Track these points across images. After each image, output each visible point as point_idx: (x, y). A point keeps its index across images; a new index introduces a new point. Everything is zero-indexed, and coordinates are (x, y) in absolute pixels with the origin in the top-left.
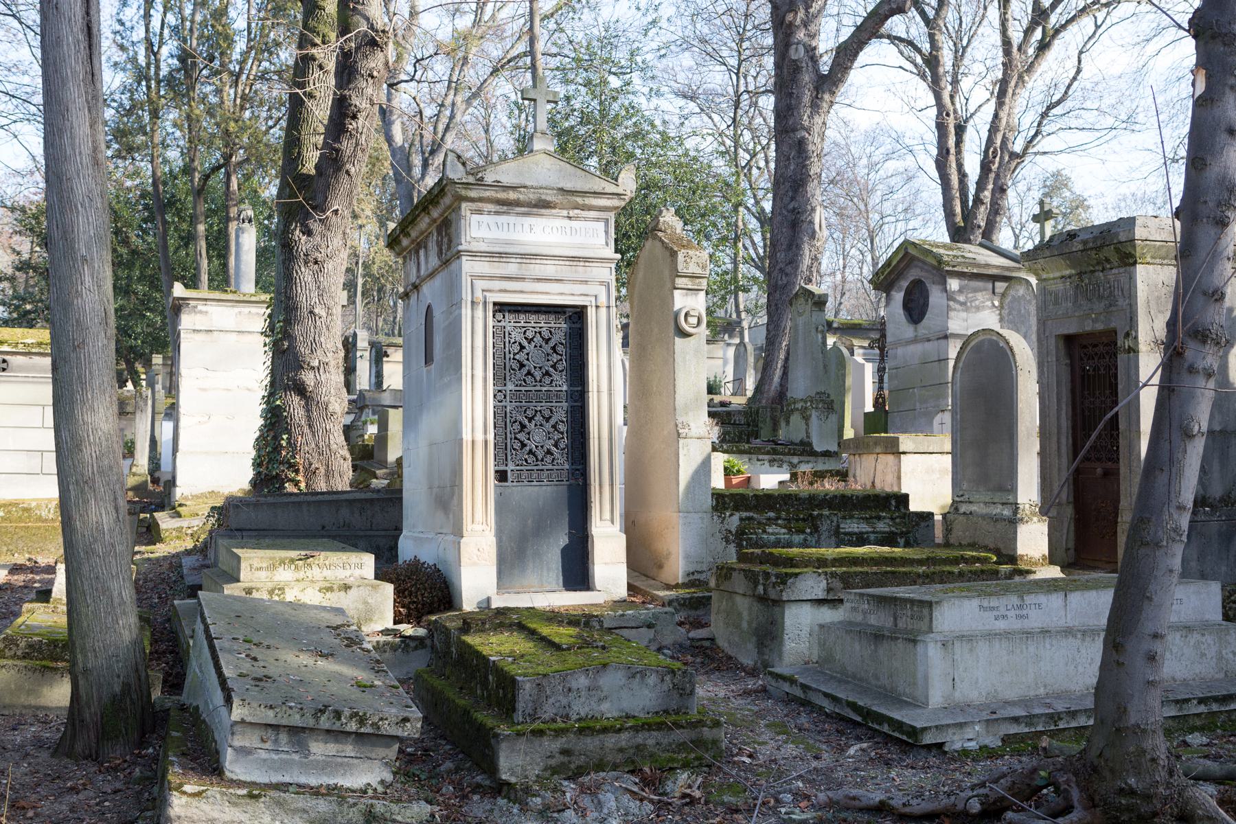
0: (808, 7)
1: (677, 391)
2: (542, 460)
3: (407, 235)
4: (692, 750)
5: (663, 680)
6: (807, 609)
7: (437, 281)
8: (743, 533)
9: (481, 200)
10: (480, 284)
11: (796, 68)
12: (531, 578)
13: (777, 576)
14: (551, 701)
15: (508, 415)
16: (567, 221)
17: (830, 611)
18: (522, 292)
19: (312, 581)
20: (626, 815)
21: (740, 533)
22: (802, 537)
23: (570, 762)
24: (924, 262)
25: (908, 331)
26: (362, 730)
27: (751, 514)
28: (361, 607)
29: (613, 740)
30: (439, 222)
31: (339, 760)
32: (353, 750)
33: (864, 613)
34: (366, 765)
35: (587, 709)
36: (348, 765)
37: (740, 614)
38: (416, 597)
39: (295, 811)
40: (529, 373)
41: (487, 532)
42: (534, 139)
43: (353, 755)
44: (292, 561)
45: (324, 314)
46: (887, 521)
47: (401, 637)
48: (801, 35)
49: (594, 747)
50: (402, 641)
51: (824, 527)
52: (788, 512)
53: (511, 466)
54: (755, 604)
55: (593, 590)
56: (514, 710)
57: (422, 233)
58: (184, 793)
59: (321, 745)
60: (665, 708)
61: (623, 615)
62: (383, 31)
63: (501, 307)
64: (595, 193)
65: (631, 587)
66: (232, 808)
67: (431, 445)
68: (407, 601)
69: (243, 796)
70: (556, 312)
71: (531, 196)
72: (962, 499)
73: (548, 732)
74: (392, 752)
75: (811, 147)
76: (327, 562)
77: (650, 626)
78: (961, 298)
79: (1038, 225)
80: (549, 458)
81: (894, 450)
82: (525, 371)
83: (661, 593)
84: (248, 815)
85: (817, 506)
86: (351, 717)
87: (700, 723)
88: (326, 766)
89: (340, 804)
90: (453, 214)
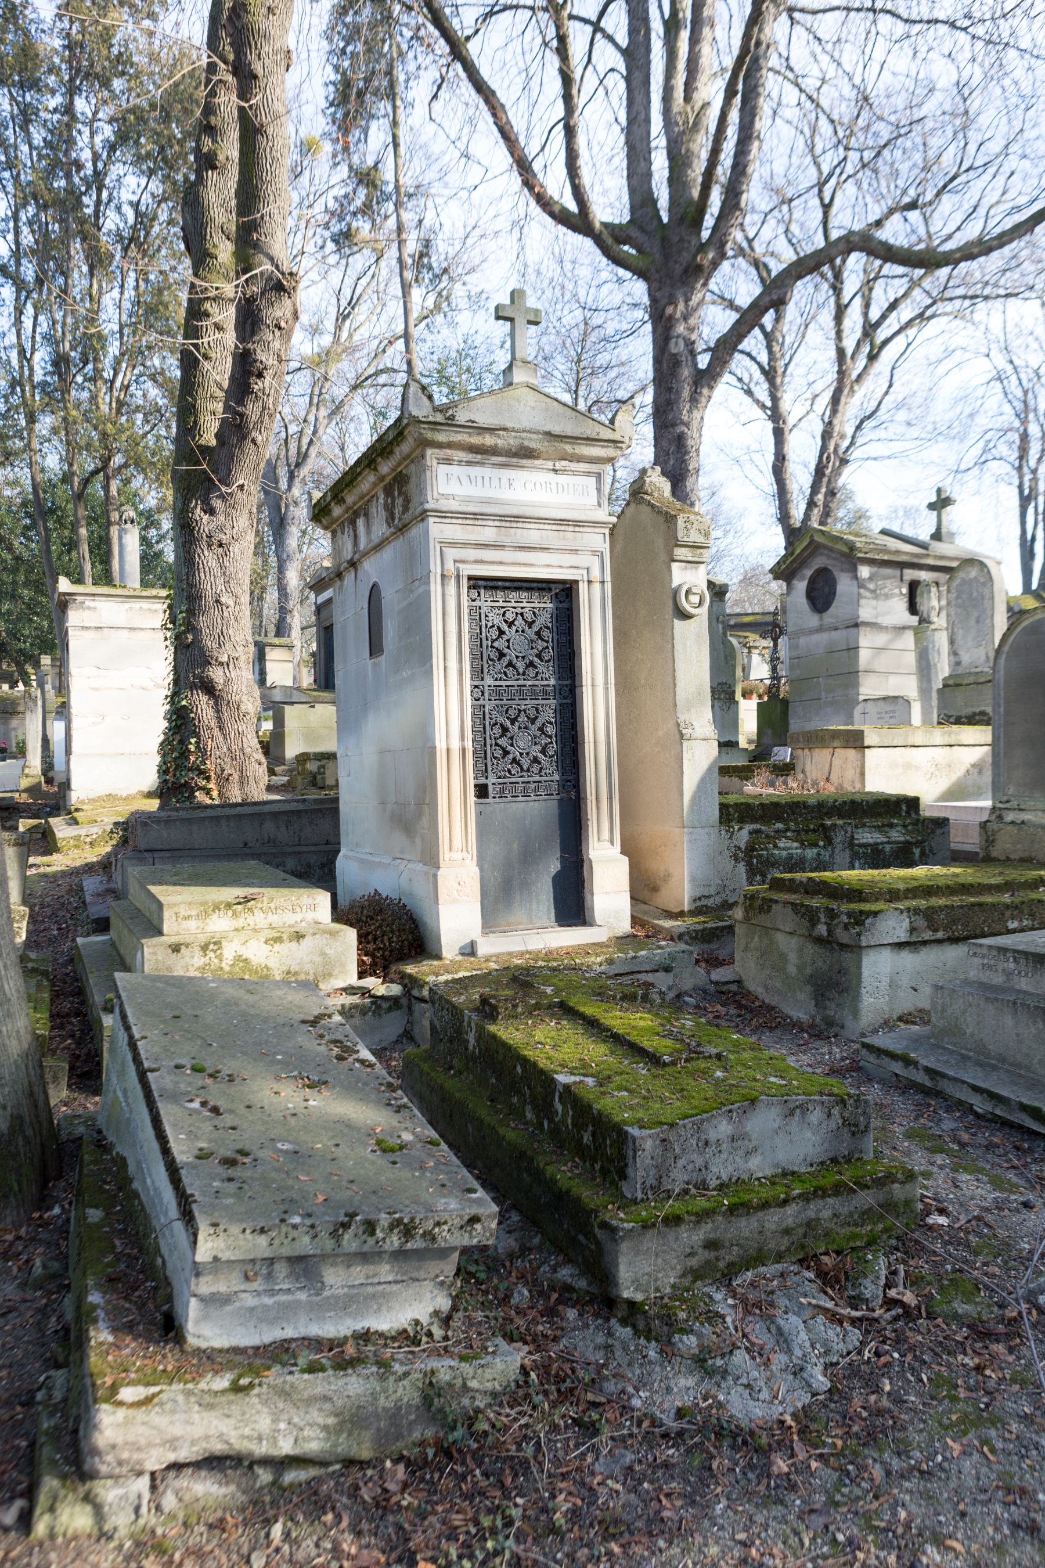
0: (687, 300)
1: (678, 684)
2: (528, 770)
3: (341, 501)
4: (881, 1218)
5: (829, 1115)
6: (886, 954)
7: (387, 554)
8: (753, 849)
9: (450, 445)
10: (451, 554)
11: (675, 363)
12: (519, 914)
13: (850, 915)
14: (681, 1163)
15: (487, 716)
16: (552, 475)
17: (911, 955)
18: (501, 563)
19: (255, 930)
20: (827, 1352)
21: (750, 849)
22: (815, 851)
23: (717, 1259)
24: (831, 550)
25: (813, 620)
26: (409, 1246)
27: (758, 826)
28: (318, 959)
29: (776, 1218)
30: (387, 480)
31: (370, 1289)
32: (391, 1271)
33: (1008, 974)
34: (410, 1291)
35: (730, 1169)
36: (384, 1295)
37: (783, 957)
38: (382, 942)
39: (310, 1401)
40: (510, 664)
41: (468, 861)
42: (514, 369)
43: (390, 1278)
44: (229, 905)
45: (231, 603)
46: (899, 828)
47: (370, 996)
48: (681, 329)
49: (751, 1232)
50: (372, 1003)
51: (838, 838)
52: (797, 823)
53: (492, 779)
54: (809, 945)
55: (591, 925)
56: (623, 1175)
57: (361, 498)
58: (121, 1404)
59: (341, 1271)
60: (832, 1155)
61: (635, 957)
62: (291, 274)
63: (477, 583)
64: (587, 439)
65: (635, 921)
66: (205, 1414)
67: (382, 752)
68: (371, 947)
69: (223, 1392)
70: (539, 589)
71: (512, 442)
72: (1008, 805)
73: (686, 1217)
74: (449, 1267)
75: (690, 442)
76: (272, 905)
77: (667, 969)
78: (871, 586)
79: (935, 513)
80: (535, 768)
81: (858, 744)
82: (505, 661)
83: (667, 924)
84: (232, 1422)
85: (826, 814)
86: (392, 1227)
87: (889, 1178)
88: (349, 1303)
89: (382, 1378)
90: (413, 467)
